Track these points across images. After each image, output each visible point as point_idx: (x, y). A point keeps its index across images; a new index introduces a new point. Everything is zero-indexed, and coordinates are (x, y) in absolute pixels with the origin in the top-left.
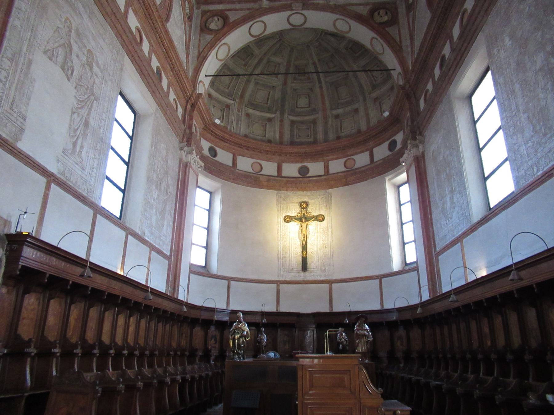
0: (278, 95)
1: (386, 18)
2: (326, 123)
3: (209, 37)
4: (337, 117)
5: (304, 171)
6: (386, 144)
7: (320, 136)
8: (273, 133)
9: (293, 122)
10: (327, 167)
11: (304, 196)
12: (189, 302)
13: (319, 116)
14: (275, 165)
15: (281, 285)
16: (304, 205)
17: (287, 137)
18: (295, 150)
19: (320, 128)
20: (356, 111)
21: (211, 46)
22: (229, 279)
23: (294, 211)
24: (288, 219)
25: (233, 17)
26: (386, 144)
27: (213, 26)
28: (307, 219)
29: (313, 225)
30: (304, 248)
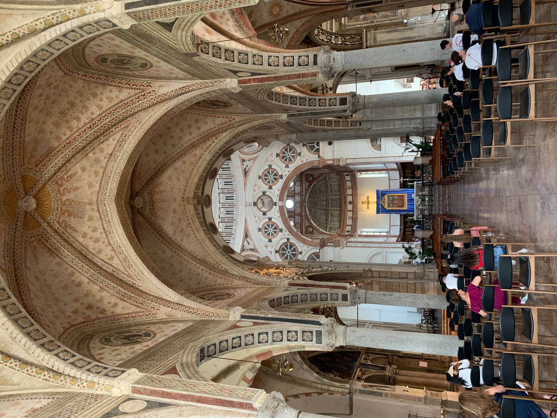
0: (322, 212)
2: (334, 195)
4: (331, 191)
5: (350, 203)
7: (338, 197)
8: (337, 213)
9: (332, 206)
12: (398, 234)
13: (330, 197)
17: (338, 209)
18: (343, 205)
19: (335, 197)
20: (330, 185)
21: (318, 231)
22: (390, 226)
23: (365, 206)
24: (368, 208)
25: (308, 224)
27: (311, 230)
29: (370, 200)
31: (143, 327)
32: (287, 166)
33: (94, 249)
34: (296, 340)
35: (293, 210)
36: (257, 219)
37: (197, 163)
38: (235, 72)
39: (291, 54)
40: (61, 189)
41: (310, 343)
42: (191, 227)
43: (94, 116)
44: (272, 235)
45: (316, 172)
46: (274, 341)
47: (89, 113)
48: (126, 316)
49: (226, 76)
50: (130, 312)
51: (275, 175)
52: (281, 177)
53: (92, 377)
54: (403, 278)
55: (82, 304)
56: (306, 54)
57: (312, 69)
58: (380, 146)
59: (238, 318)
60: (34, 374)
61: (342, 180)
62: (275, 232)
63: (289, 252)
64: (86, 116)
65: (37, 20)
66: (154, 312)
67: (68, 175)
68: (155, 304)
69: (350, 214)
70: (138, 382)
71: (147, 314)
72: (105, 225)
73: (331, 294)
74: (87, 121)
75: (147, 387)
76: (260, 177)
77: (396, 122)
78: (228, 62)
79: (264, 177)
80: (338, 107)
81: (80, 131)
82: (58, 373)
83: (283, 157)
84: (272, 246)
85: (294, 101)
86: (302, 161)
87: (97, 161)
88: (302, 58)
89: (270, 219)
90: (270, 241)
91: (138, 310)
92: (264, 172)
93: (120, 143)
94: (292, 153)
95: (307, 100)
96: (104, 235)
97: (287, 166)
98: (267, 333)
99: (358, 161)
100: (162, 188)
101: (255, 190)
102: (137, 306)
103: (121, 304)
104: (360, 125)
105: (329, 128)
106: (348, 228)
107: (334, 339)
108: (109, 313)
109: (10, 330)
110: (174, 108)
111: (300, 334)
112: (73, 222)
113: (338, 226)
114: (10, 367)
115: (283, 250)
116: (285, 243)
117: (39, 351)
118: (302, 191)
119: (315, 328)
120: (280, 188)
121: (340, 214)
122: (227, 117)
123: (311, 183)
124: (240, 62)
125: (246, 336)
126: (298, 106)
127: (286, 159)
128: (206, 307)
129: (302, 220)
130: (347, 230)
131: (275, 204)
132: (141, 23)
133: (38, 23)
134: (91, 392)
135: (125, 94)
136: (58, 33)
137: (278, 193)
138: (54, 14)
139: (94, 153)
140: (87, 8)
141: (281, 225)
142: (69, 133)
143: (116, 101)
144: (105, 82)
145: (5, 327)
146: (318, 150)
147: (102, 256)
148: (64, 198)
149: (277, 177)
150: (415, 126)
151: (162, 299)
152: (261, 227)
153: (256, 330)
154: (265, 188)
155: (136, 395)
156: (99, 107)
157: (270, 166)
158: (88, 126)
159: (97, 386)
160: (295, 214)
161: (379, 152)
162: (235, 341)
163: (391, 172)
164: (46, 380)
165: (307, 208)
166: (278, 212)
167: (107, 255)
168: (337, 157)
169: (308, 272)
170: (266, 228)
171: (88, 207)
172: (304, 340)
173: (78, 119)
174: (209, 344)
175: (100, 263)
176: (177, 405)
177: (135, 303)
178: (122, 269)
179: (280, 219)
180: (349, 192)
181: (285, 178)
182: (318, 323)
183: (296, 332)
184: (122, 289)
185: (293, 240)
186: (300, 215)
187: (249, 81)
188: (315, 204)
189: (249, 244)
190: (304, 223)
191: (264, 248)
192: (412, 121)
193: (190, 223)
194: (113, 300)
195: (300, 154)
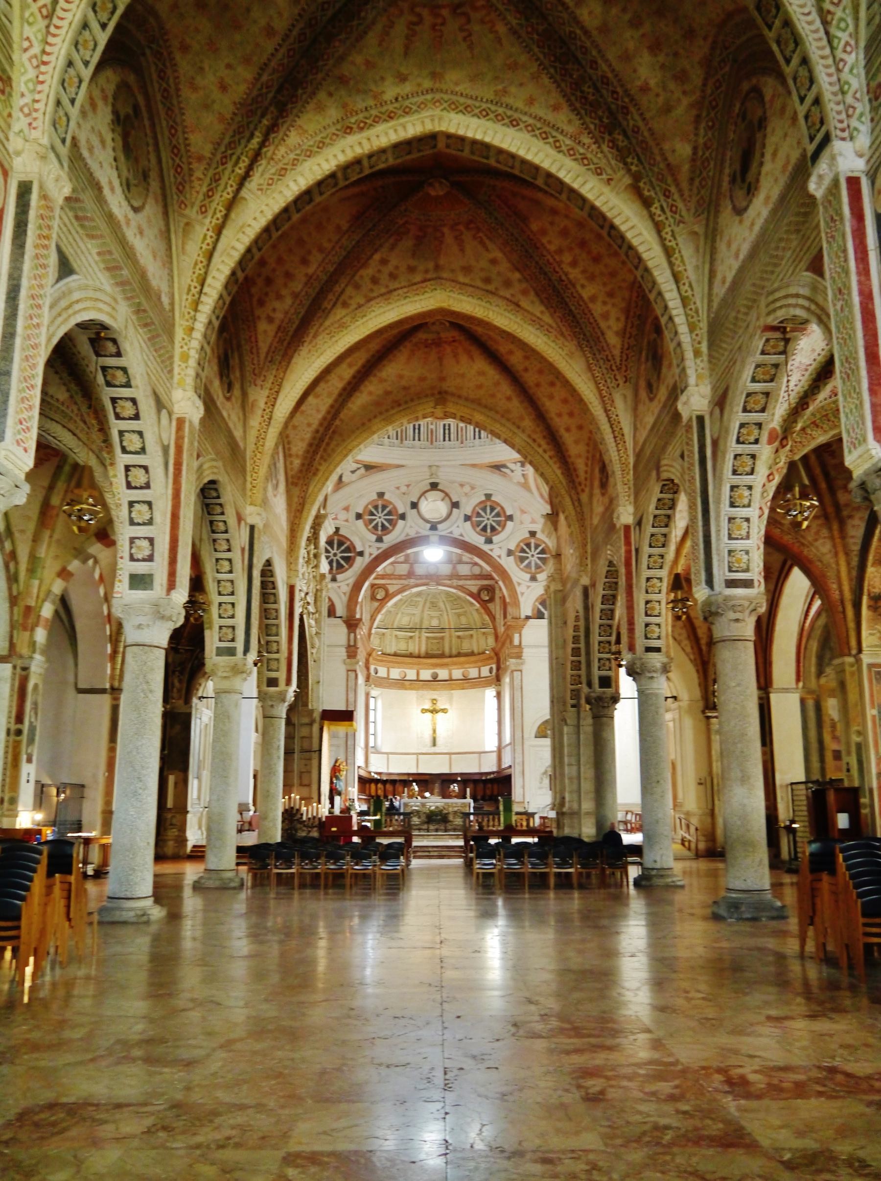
0: (417, 619)
1: (487, 598)
2: (451, 641)
3: (376, 604)
4: (459, 637)
5: (435, 678)
6: (488, 668)
8: (413, 648)
10: (450, 674)
11: (434, 694)
13: (446, 635)
14: (415, 671)
15: (421, 756)
16: (434, 701)
21: (378, 610)
22: (387, 753)
23: (428, 706)
24: (424, 711)
25: (392, 589)
26: (488, 668)
27: (379, 597)
28: (437, 712)
29: (440, 714)
30: (434, 731)
31: (238, 374)
32: (510, 553)
33: (361, 277)
34: (220, 617)
35: (421, 560)
36: (404, 489)
37: (508, 420)
38: (639, 523)
39: (664, 611)
40: (461, 227)
41: (216, 638)
42: (393, 408)
43: (579, 288)
44: (371, 521)
45: (498, 608)
46: (219, 582)
47: (583, 281)
48: (253, 339)
49: (636, 508)
50: (261, 344)
51: (493, 529)
52: (489, 541)
53: (194, 355)
54: (301, 778)
55: (274, 270)
56: (663, 634)
57: (640, 643)
58: (545, 737)
59: (250, 520)
60: (197, 272)
61: (482, 661)
62: (376, 527)
63: (335, 555)
64: (580, 276)
65: (691, 286)
66: (259, 382)
67: (484, 238)
68: (271, 381)
69: (411, 674)
70: (190, 422)
71: (257, 371)
72: (400, 291)
73: (277, 660)
74: (571, 277)
75: (186, 440)
76: (488, 496)
77: (575, 768)
78: (651, 518)
79: (489, 504)
80: (596, 673)
81: (555, 265)
82: (197, 303)
83: (528, 545)
84: (347, 521)
85: (608, 600)
86: (519, 584)
87: (508, 284)
88: (656, 629)
89: (403, 517)
90: (359, 516)
91: (262, 356)
92: (498, 504)
93: (536, 321)
94: (536, 564)
95: (609, 622)
96: (383, 290)
97: (510, 553)
98: (231, 572)
99: (518, 694)
100: (464, 358)
101: (462, 485)
102: (267, 353)
103: (271, 329)
104: (573, 706)
105: (569, 651)
106: (382, 672)
107: (225, 674)
108: (258, 312)
109: (253, 223)
110: (592, 414)
111: (230, 622)
112: (408, 243)
113: (388, 651)
114: (205, 235)
115: (340, 544)
116: (354, 548)
117: (227, 271)
118: (460, 577)
119: (240, 645)
120: (467, 539)
121: (411, 656)
122: (586, 479)
123: (477, 596)
124: (652, 535)
125: (228, 540)
126: (598, 606)
127: (526, 552)
128: (266, 466)
129: (400, 577)
130: (379, 669)
131: (434, 527)
132: (684, 430)
133: (687, 287)
134: (177, 359)
135: (613, 340)
136: (674, 312)
137: (456, 534)
138: (697, 312)
139: (520, 281)
140: (702, 361)
141: (390, 539)
142: (552, 248)
143: (603, 324)
144: (632, 314)
145: (258, 215)
146: (540, 616)
147: (350, 290)
148: (446, 230)
149: (489, 532)
150: (567, 799)
151: (278, 392)
152: (386, 497)
153: (236, 555)
154: (467, 508)
155: (174, 423)
156: (593, 299)
157: (510, 518)
158: (564, 278)
159: (183, 365)
160: (412, 565)
161: (533, 735)
162: (221, 524)
163: (494, 756)
164: (189, 290)
165: (424, 588)
166: (417, 533)
167: (351, 297)
168: (527, 653)
169: (309, 613)
170: (384, 507)
171: (431, 265)
172: (221, 627)
173: (574, 264)
174: (221, 490)
175: (338, 289)
176: (167, 488)
177: (273, 349)
178: (327, 323)
179: (402, 538)
180: (457, 674)
181: (486, 548)
182: (246, 650)
183: (233, 617)
184: (294, 326)
185: (360, 563)
186: (410, 574)
187: (628, 543)
188: (434, 605)
189: (353, 472)
190: (394, 582)
191: (344, 504)
192: (575, 796)
193: (399, 405)
194: (279, 316)
195: (533, 579)
